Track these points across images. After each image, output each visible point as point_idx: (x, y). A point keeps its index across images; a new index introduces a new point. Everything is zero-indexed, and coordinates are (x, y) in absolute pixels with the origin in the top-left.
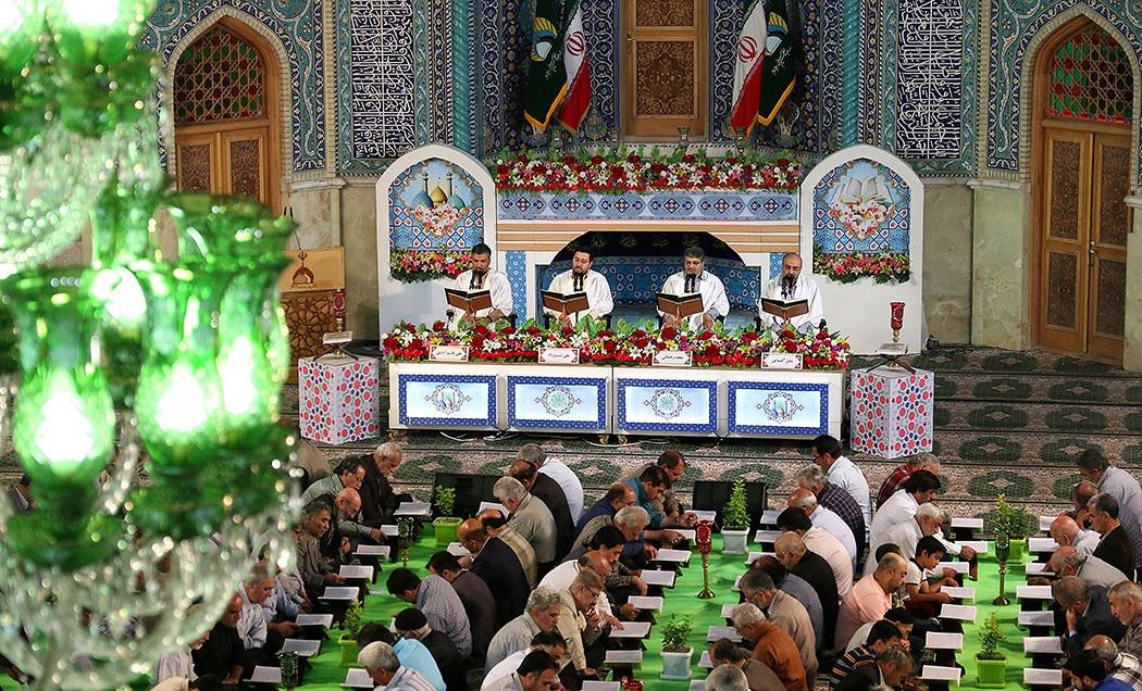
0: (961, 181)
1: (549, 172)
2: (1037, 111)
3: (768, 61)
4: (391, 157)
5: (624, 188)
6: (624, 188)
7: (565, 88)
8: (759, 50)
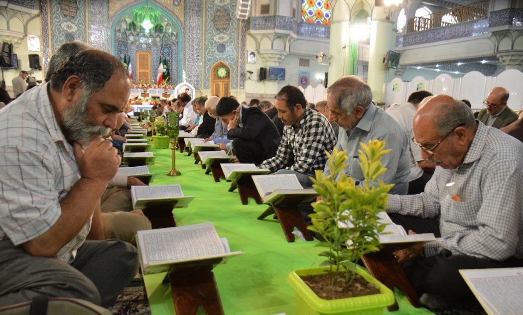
3: (164, 73)
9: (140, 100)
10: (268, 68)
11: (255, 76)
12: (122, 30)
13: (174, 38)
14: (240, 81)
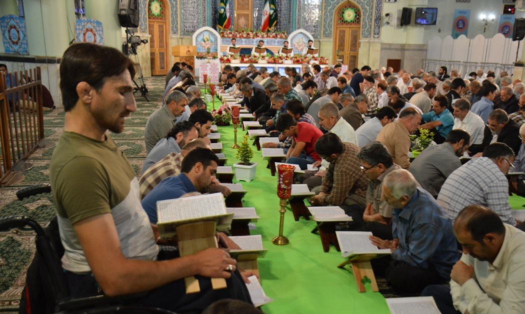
0: (318, 40)
1: (233, 34)
2: (335, 24)
3: (270, 16)
4: (193, 32)
5: (250, 37)
6: (250, 37)
7: (226, 20)
8: (268, 14)
9: (255, 57)
10: (414, 8)
11: (395, 21)
14: (375, 28)
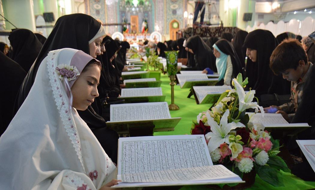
12: (123, 5)
13: (149, 8)
